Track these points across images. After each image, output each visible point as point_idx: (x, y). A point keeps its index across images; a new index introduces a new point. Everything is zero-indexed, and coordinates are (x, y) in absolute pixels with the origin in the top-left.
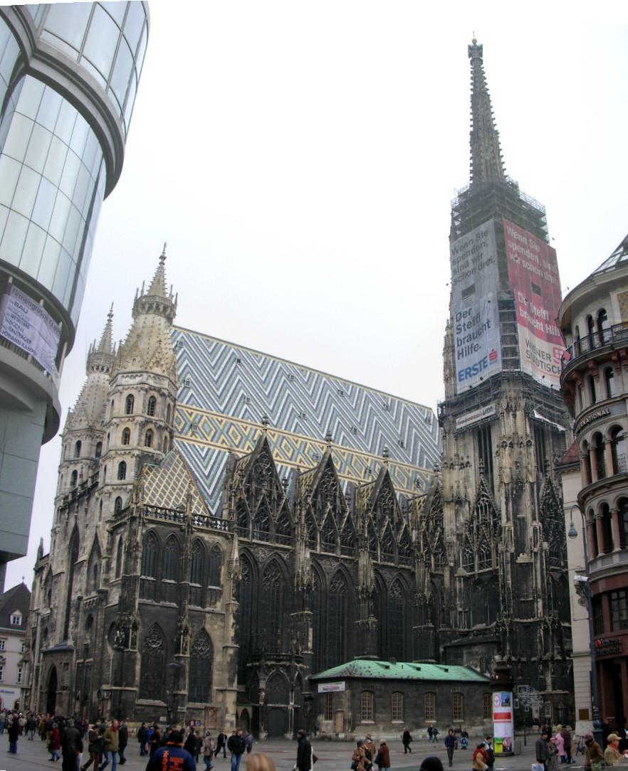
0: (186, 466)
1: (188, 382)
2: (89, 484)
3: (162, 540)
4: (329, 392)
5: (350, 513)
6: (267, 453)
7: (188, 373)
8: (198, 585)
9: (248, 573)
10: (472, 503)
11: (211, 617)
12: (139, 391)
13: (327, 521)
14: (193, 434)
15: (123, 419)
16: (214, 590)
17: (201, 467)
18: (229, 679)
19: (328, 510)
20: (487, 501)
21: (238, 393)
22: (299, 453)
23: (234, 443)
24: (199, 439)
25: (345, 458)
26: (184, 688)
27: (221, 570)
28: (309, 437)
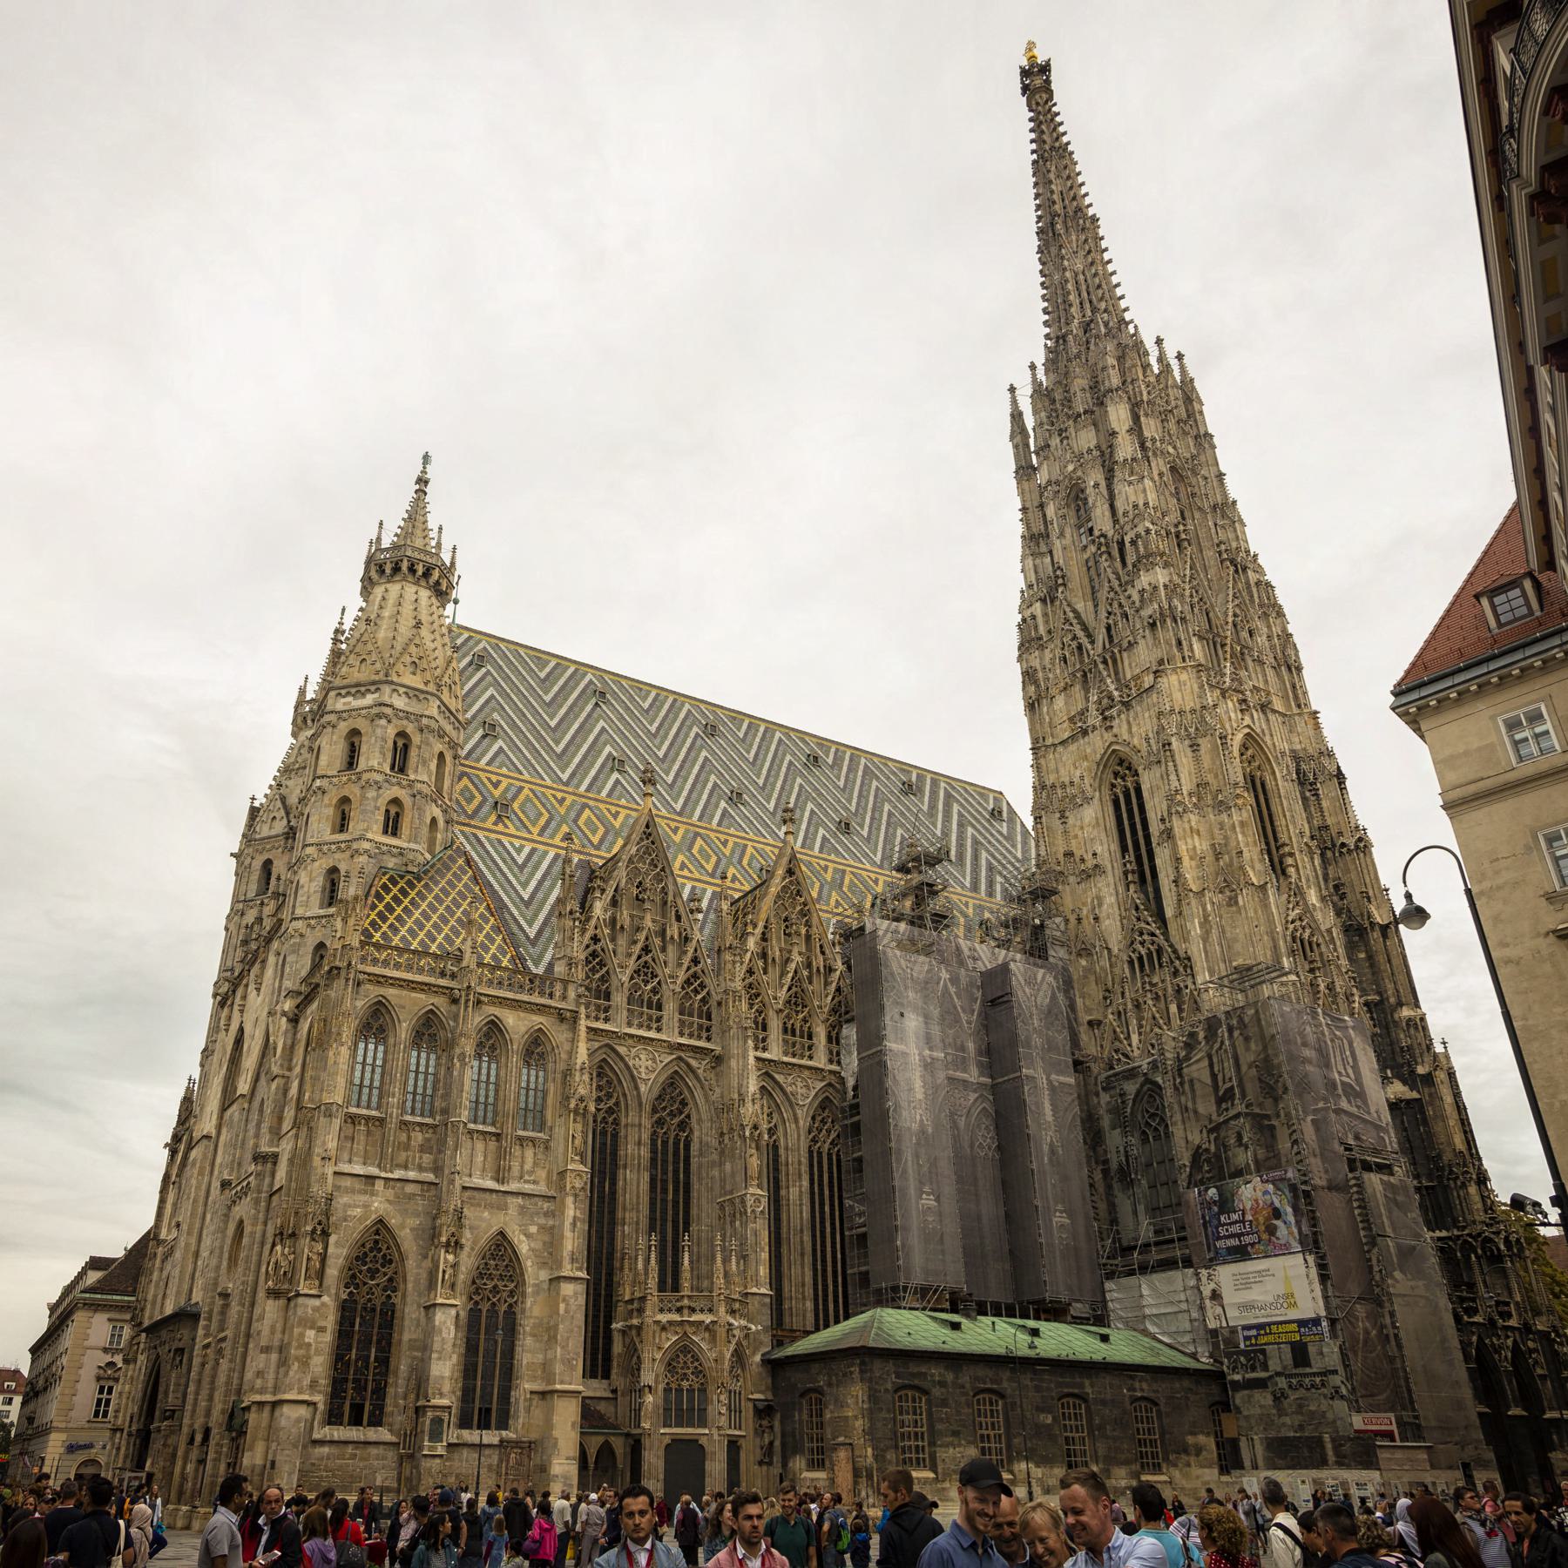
0: (477, 878)
6: (653, 843)
9: (617, 1104)
10: (1115, 951)
13: (794, 989)
17: (514, 882)
19: (793, 966)
20: (1153, 943)
21: (600, 752)
22: (730, 863)
23: (590, 841)
24: (512, 830)
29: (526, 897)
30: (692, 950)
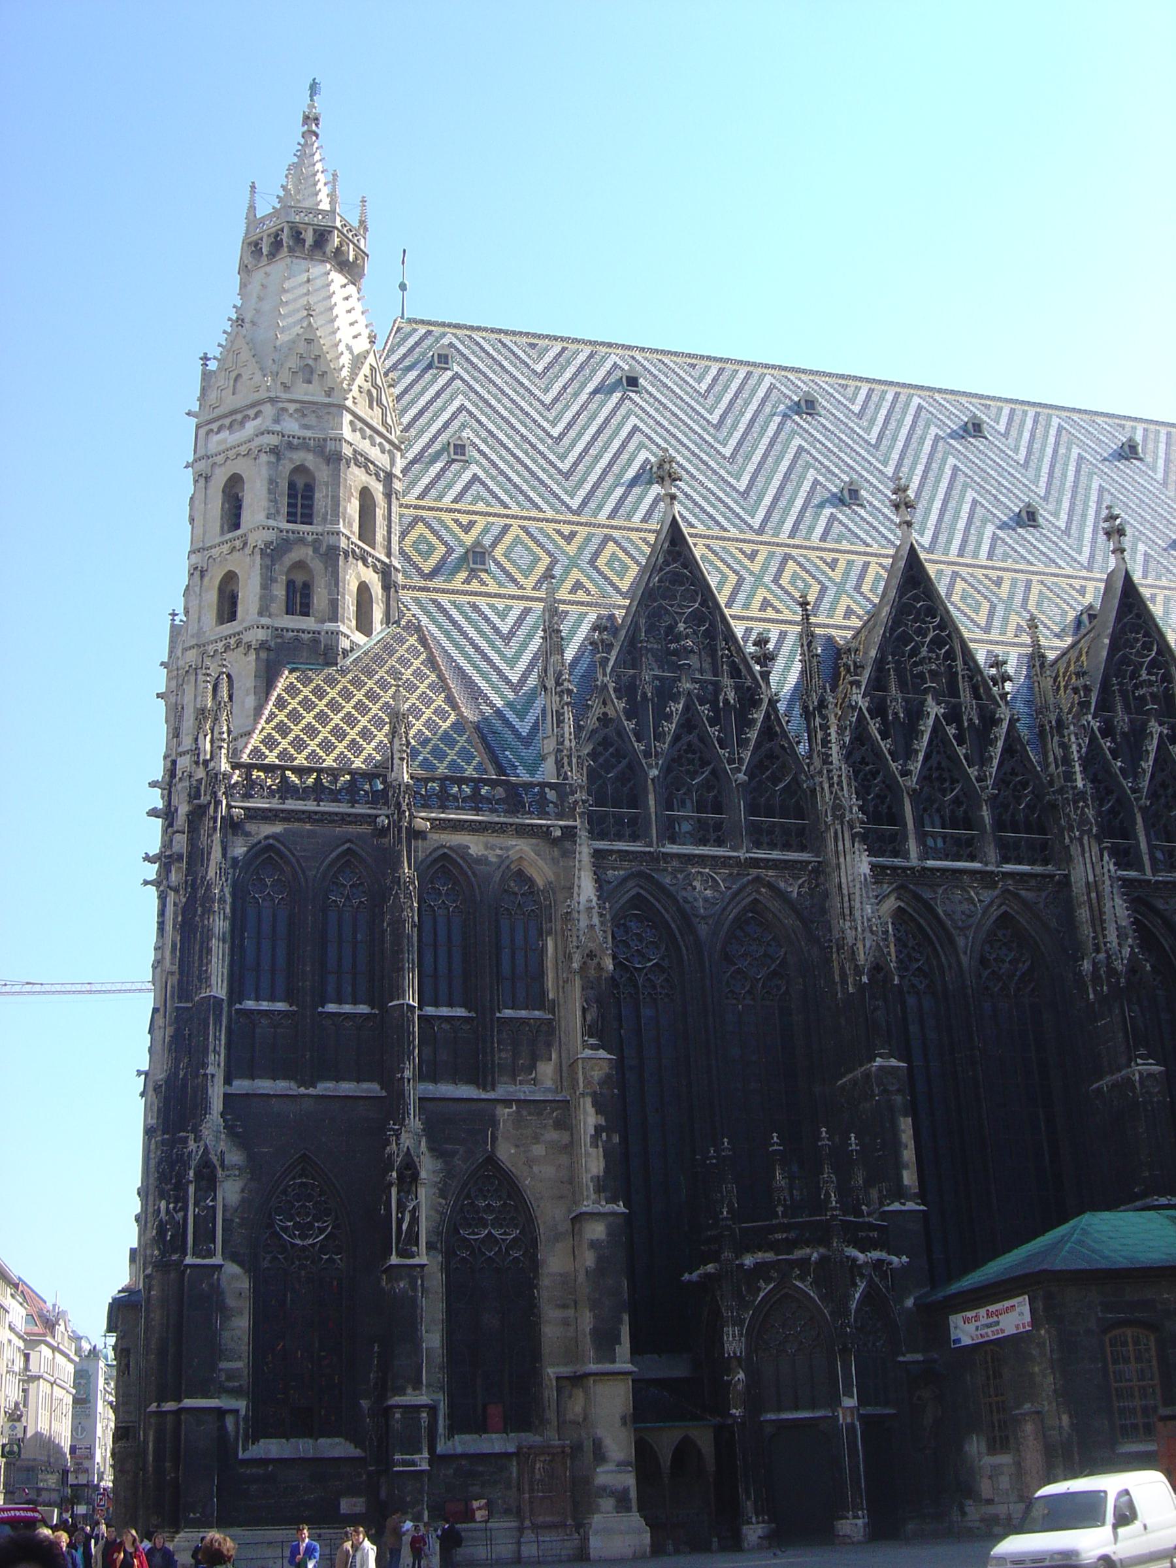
1: (460, 449)
3: (311, 874)
5: (1012, 722)
7: (463, 426)
8: (460, 1012)
11: (518, 1112)
15: (215, 552)
16: (523, 1021)
18: (595, 1332)
19: (931, 722)
24: (493, 588)
26: (417, 1384)
27: (543, 951)
28: (875, 548)
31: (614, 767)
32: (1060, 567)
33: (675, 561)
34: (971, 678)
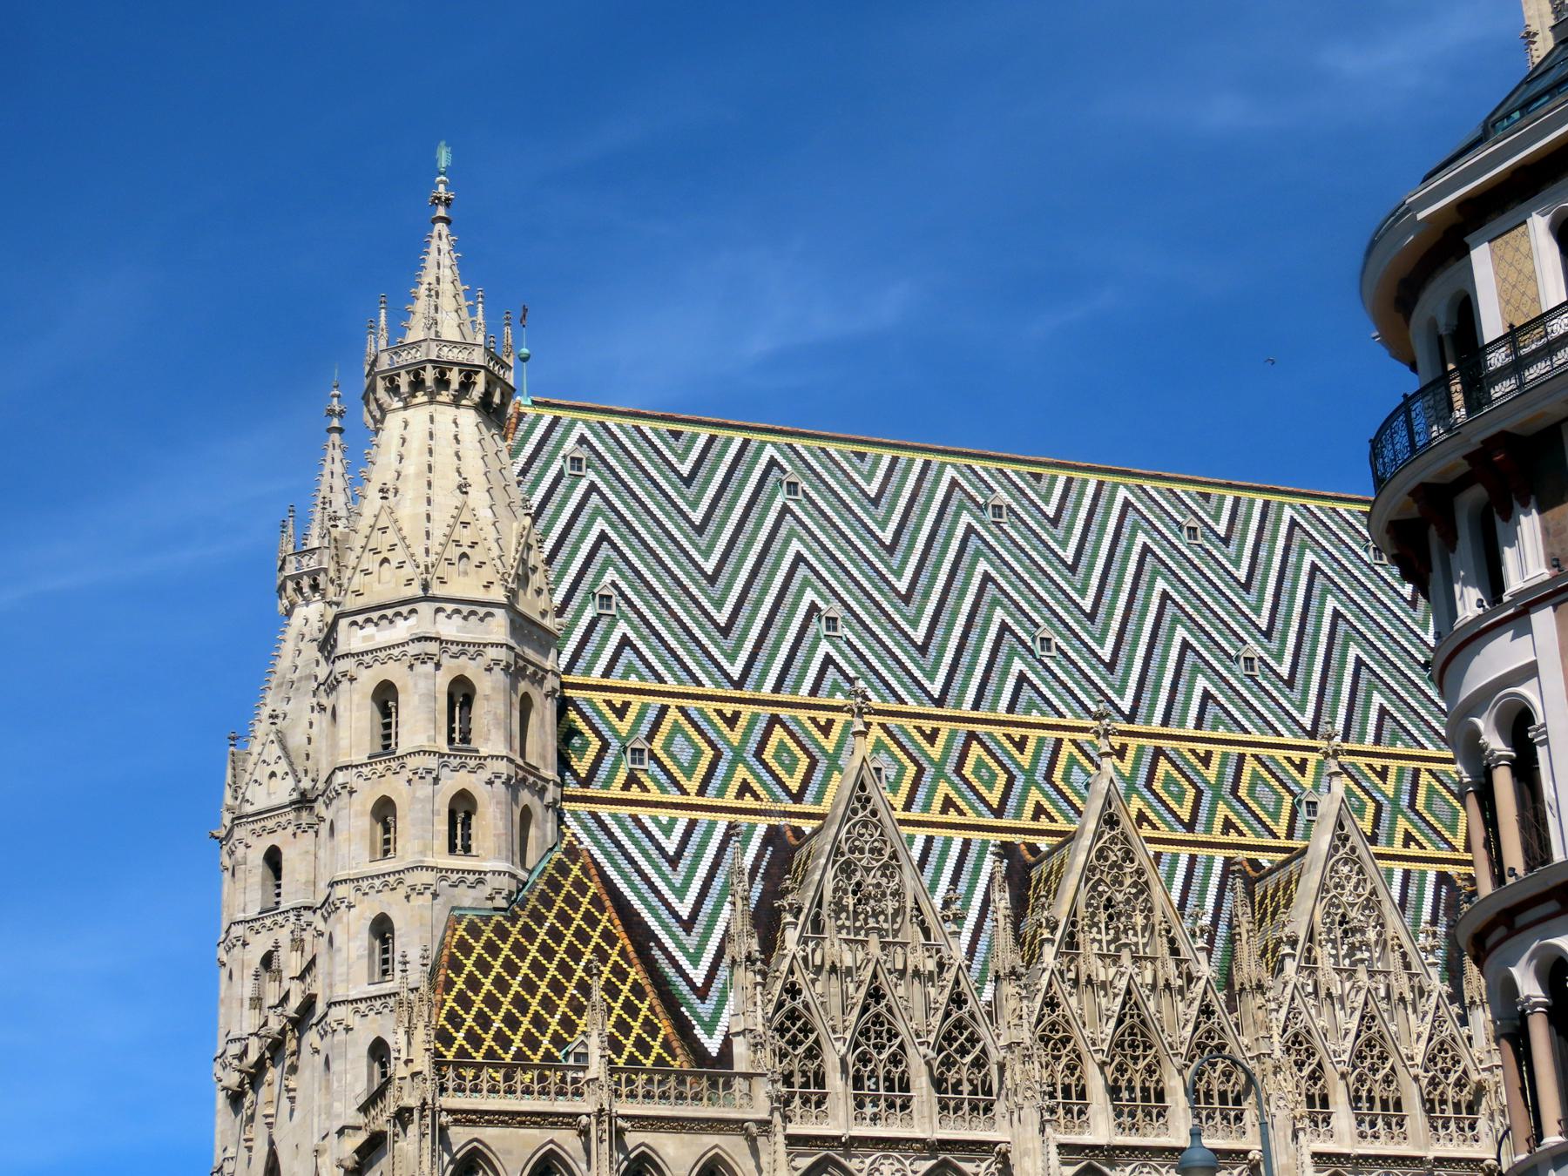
2: (295, 1002)
4: (1141, 538)
7: (608, 562)
12: (411, 667)
13: (1128, 1020)
14: (632, 780)
15: (365, 770)
19: (1122, 984)
22: (1030, 782)
24: (655, 795)
25: (1211, 774)
28: (1070, 720)
29: (685, 913)
30: (951, 984)
31: (801, 1043)
32: (1280, 735)
33: (864, 808)
34: (1168, 931)
